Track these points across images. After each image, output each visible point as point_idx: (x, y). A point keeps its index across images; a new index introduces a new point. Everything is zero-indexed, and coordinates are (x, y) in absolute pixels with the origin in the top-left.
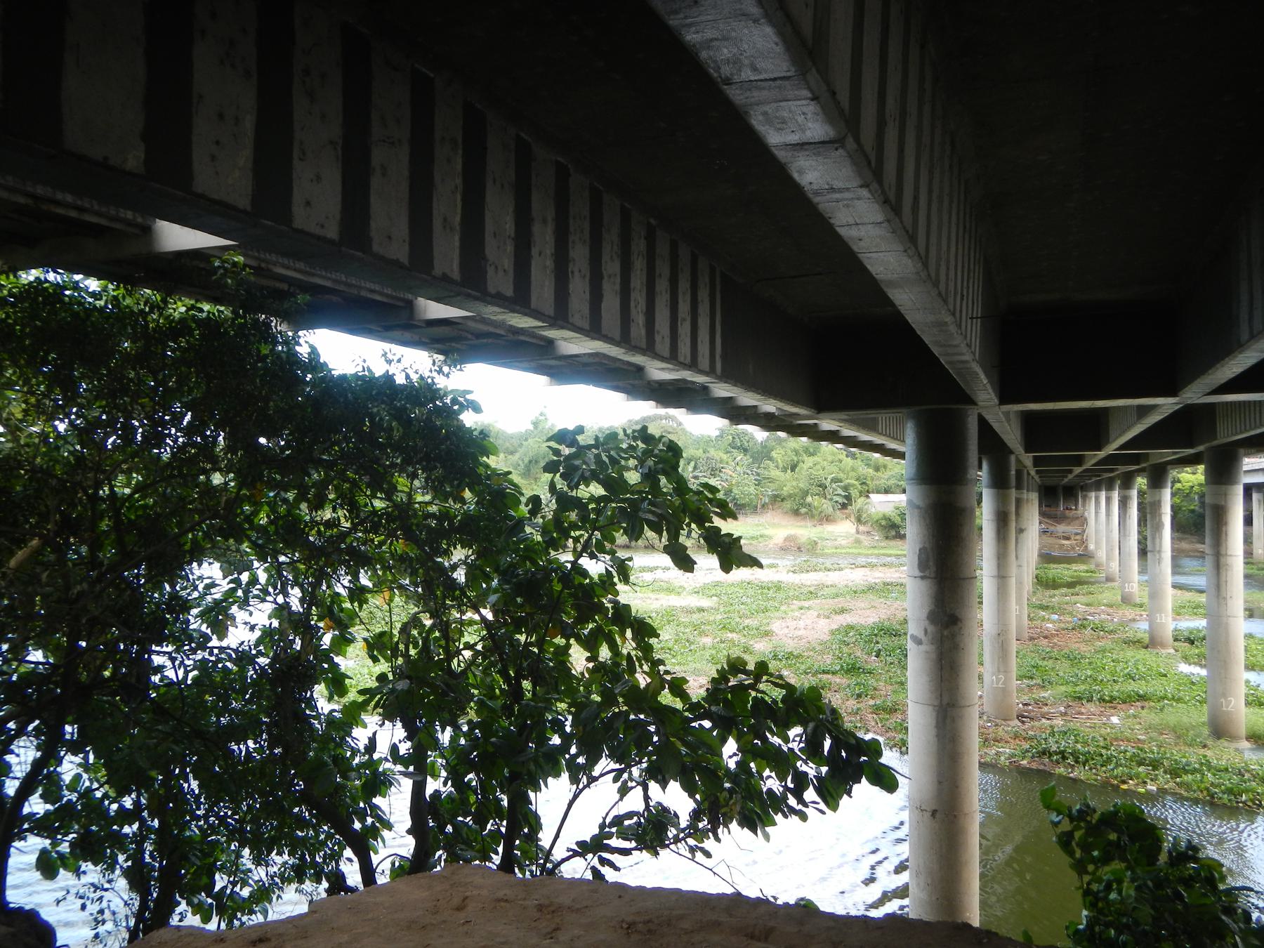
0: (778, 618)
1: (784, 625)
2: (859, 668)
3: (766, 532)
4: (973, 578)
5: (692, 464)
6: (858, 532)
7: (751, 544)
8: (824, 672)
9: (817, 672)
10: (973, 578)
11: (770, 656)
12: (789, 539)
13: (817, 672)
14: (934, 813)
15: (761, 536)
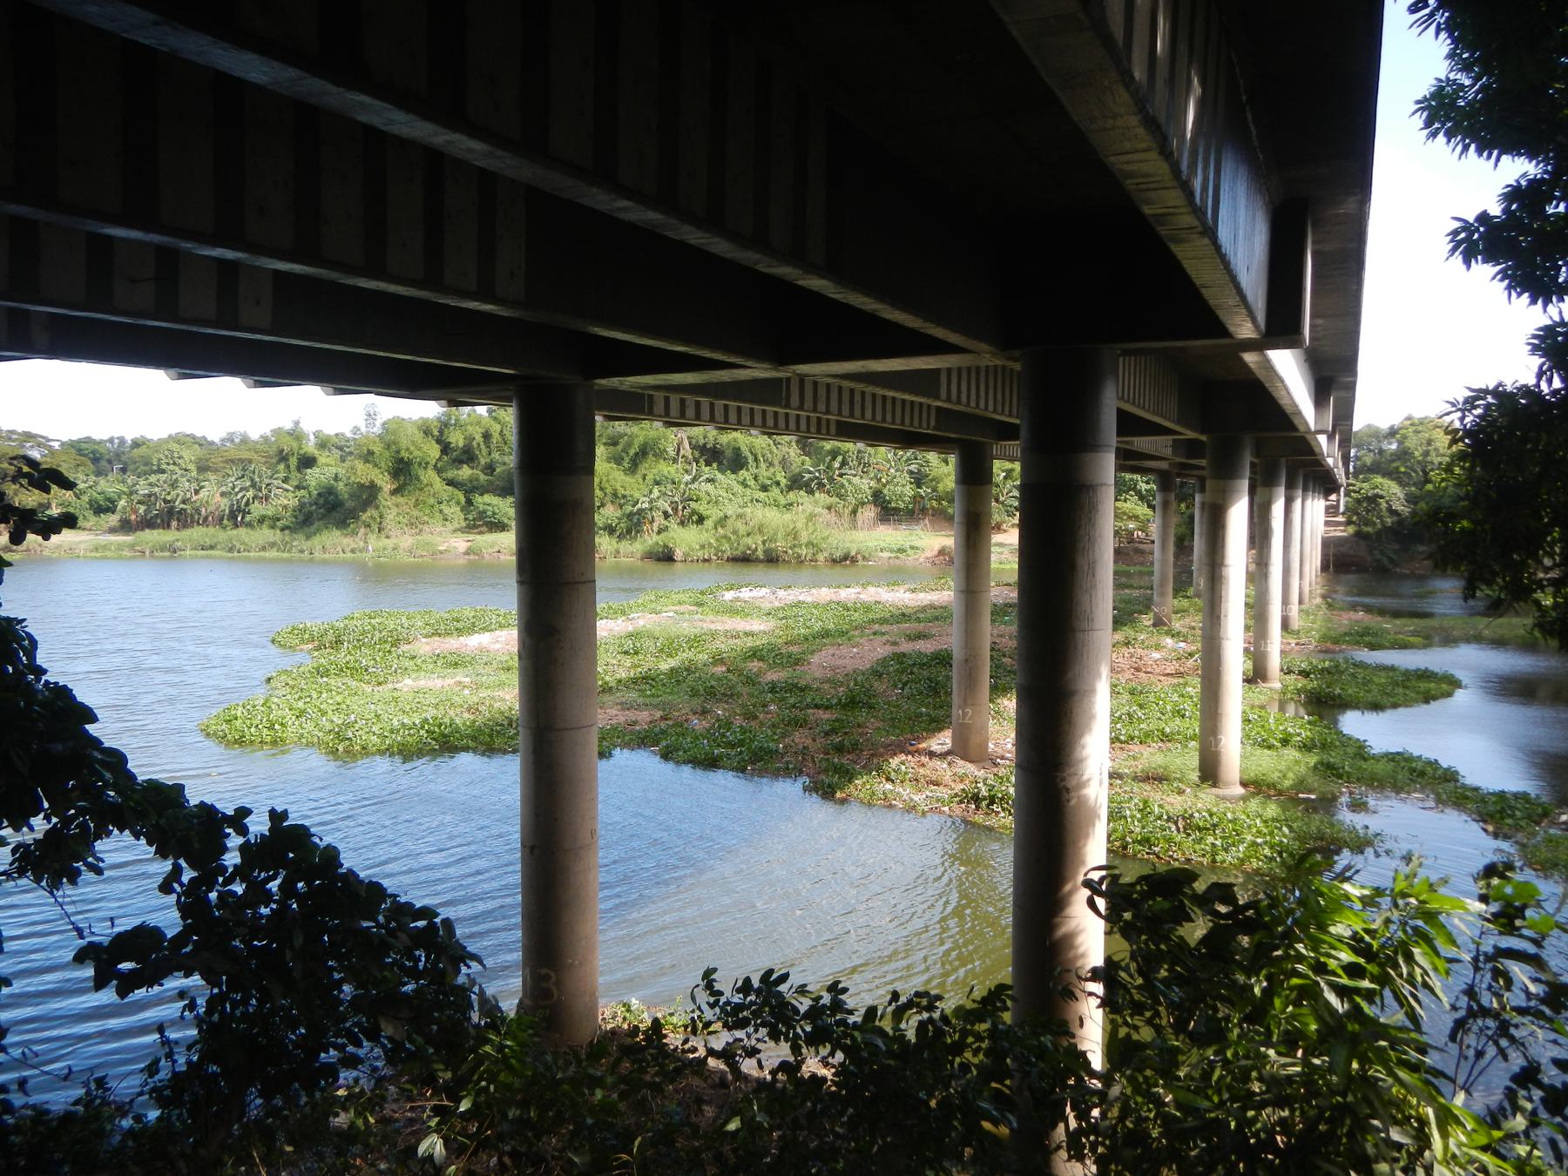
0: (833, 645)
1: (831, 652)
2: (859, 702)
3: (917, 544)
4: (579, 583)
5: (840, 458)
7: (898, 558)
8: (817, 707)
9: (808, 706)
10: (579, 583)
11: (766, 688)
12: (942, 552)
13: (808, 706)
14: (532, 848)
15: (912, 548)
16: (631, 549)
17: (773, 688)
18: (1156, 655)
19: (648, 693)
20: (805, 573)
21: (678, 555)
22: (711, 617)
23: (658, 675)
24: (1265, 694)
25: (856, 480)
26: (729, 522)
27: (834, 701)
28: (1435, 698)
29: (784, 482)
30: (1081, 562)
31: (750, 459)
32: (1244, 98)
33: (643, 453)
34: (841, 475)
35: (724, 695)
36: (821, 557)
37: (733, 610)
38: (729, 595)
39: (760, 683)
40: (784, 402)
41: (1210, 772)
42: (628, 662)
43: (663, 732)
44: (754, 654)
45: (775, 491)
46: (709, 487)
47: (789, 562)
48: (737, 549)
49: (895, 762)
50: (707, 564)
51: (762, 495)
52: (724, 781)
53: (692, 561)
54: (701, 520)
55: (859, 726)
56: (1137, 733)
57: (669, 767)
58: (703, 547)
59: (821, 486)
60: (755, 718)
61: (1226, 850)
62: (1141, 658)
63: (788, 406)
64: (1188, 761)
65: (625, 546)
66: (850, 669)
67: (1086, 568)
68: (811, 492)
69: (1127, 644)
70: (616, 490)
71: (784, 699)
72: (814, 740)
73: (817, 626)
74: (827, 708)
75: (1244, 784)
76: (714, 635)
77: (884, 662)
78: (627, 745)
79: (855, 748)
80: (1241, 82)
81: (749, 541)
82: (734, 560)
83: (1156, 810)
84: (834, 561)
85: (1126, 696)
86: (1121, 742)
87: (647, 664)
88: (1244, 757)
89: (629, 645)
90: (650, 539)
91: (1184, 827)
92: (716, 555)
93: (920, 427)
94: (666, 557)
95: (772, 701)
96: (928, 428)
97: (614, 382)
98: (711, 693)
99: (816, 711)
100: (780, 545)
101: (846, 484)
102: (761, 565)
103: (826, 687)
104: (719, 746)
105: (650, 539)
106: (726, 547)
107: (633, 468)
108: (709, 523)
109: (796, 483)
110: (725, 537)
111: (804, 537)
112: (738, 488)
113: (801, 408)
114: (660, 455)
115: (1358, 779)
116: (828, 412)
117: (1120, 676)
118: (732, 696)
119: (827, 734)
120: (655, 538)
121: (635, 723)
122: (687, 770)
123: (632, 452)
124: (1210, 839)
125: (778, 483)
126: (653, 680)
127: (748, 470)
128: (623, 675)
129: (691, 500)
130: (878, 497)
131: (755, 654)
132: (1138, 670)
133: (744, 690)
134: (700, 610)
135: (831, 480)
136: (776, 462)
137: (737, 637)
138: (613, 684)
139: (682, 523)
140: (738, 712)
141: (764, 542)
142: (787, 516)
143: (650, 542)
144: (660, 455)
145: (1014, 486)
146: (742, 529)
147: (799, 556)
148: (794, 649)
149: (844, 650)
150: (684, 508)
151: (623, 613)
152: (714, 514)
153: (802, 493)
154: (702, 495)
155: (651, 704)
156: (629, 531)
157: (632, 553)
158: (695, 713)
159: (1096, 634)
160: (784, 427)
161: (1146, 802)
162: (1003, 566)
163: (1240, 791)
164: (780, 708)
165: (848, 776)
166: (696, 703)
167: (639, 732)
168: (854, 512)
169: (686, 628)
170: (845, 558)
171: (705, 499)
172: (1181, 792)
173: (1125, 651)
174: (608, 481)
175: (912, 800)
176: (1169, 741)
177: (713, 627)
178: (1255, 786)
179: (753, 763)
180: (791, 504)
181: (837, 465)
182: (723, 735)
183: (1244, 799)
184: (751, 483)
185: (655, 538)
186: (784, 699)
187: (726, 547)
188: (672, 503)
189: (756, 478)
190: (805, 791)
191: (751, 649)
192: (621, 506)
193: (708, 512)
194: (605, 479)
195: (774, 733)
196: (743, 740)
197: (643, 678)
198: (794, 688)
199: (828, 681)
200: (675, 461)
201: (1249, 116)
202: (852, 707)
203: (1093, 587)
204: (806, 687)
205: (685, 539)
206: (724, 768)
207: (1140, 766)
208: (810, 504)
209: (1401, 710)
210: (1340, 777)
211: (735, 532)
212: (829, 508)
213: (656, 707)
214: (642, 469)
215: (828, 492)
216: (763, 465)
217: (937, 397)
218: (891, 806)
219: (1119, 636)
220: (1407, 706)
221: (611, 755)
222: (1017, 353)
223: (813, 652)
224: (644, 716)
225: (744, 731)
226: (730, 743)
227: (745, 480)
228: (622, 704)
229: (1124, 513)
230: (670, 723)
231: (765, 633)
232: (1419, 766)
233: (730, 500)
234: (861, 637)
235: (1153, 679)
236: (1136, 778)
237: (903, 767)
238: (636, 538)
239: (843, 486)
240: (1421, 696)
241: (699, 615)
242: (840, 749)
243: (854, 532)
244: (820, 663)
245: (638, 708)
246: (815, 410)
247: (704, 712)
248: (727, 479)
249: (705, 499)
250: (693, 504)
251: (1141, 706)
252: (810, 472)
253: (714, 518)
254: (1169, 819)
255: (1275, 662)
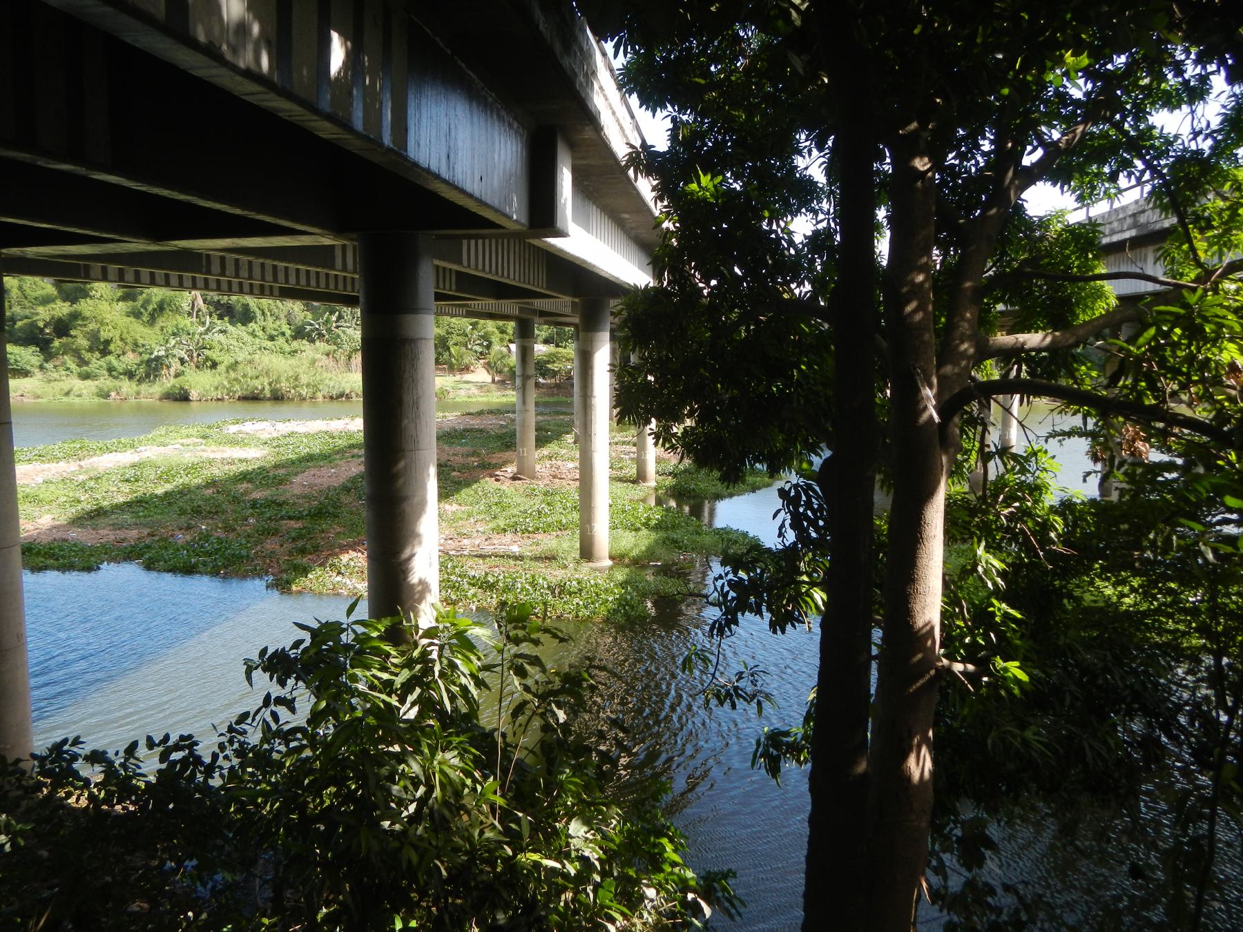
1: (312, 473)
6: (493, 381)
8: (290, 518)
9: (282, 518)
16: (151, 390)
17: (254, 504)
18: (571, 465)
19: (141, 514)
20: (306, 406)
21: (194, 394)
22: (213, 447)
23: (152, 498)
24: (644, 491)
25: (350, 331)
26: (240, 367)
27: (306, 512)
28: (759, 488)
29: (288, 333)
30: (407, 398)
31: (258, 313)
32: (449, 52)
33: (161, 308)
34: (337, 327)
35: (210, 512)
36: (320, 395)
37: (233, 442)
38: (233, 429)
39: (244, 501)
40: (204, 270)
41: (587, 552)
42: (126, 488)
43: (148, 547)
44: (245, 477)
45: (281, 340)
46: (221, 337)
47: (292, 400)
48: (247, 390)
49: (345, 558)
50: (220, 403)
51: (269, 344)
52: (202, 587)
53: (206, 400)
54: (214, 365)
55: (323, 531)
56: (541, 525)
57: (154, 574)
58: (217, 388)
59: (321, 336)
60: (234, 530)
61: (586, 607)
62: (558, 469)
63: (209, 272)
64: (569, 544)
65: (144, 387)
66: (325, 486)
67: (411, 403)
68: (312, 341)
69: (550, 458)
70: (136, 340)
71: (262, 513)
72: (282, 546)
73: (304, 451)
74: (299, 519)
75: (612, 558)
76: (211, 462)
77: (353, 480)
78: (114, 560)
79: (316, 549)
80: (437, 39)
81: (257, 383)
82: (244, 398)
83: (541, 581)
84: (331, 398)
85: (541, 497)
86: (529, 532)
87: (142, 489)
88: (613, 539)
89: (130, 473)
90: (167, 382)
91: (560, 593)
92: (228, 395)
93: (345, 290)
94: (183, 397)
95: (252, 515)
96: (353, 291)
97: (15, 251)
98: (197, 511)
99: (288, 521)
100: (284, 385)
101: (342, 335)
102: (268, 405)
103: (301, 501)
104: (197, 555)
105: (167, 382)
106: (237, 387)
107: (152, 320)
108: (221, 368)
110: (236, 379)
111: (304, 379)
113: (223, 274)
114: (178, 310)
115: (693, 549)
116: (250, 278)
117: (540, 483)
118: (217, 512)
119: (294, 540)
120: (173, 381)
121: (124, 540)
122: (168, 577)
123: (150, 308)
124: (576, 600)
125: (283, 334)
126: (147, 503)
127: (256, 322)
128: (121, 499)
129: (205, 348)
131: (245, 477)
132: (554, 477)
133: (229, 508)
134: (204, 442)
135: (329, 331)
136: (282, 316)
137: (232, 463)
138: (108, 508)
139: (197, 367)
140: (220, 525)
141: (270, 384)
142: (293, 361)
143: (169, 385)
144: (178, 310)
145: (482, 337)
146: (250, 372)
147: (300, 395)
148: (281, 472)
149: (324, 471)
150: (199, 355)
151: (132, 446)
152: (227, 360)
153: (304, 342)
154: (215, 344)
155: (141, 524)
156: (148, 376)
157: (151, 394)
158: (181, 529)
159: (421, 452)
160: (227, 289)
161: (533, 577)
162: (470, 400)
163: (610, 563)
164: (257, 521)
165: (305, 571)
166: (183, 520)
167: (126, 548)
168: (350, 357)
169: (188, 458)
170: (341, 395)
171: (218, 347)
172: (565, 567)
173: (548, 463)
174: (128, 333)
175: (355, 588)
176: (565, 529)
177: (212, 456)
178: (617, 558)
179: (226, 567)
180: (296, 351)
181: (334, 318)
182: (202, 547)
183: (611, 568)
184: (260, 333)
185: (173, 381)
186: (262, 513)
187: (237, 387)
188: (187, 351)
189: (264, 329)
190: (267, 587)
191: (241, 473)
192: (141, 354)
193: (221, 359)
194: (125, 331)
195: (248, 542)
196: (220, 549)
197: (138, 502)
198: (272, 503)
199: (305, 497)
200: (190, 314)
201: (463, 65)
202: (320, 518)
203: (418, 417)
204: (284, 502)
205: (199, 382)
206: (201, 573)
207: (538, 551)
208: (311, 351)
209: (735, 498)
210: (680, 548)
211: (245, 376)
212: (328, 355)
213: (145, 526)
214: (161, 322)
215: (327, 342)
216: (270, 319)
217: (333, 268)
218: (338, 594)
219: (545, 451)
220: (739, 495)
221: (99, 568)
222: (354, 236)
223: (296, 474)
224: (134, 533)
225: (219, 540)
226: (207, 552)
227: (254, 331)
228: (113, 525)
229: (563, 357)
230: (156, 538)
231: (258, 459)
232: (733, 537)
233: (241, 348)
234: (341, 459)
235: (564, 482)
236: (537, 559)
237: (352, 563)
238: (154, 382)
239: (339, 336)
240: (750, 487)
241: (203, 447)
242: (303, 551)
243: (349, 374)
244: (300, 483)
245: (129, 527)
246: (237, 276)
247: (189, 528)
248: (237, 331)
249: (218, 347)
250: (207, 352)
251: (548, 504)
252: (311, 325)
253: (226, 363)
254: (549, 588)
255: (651, 468)
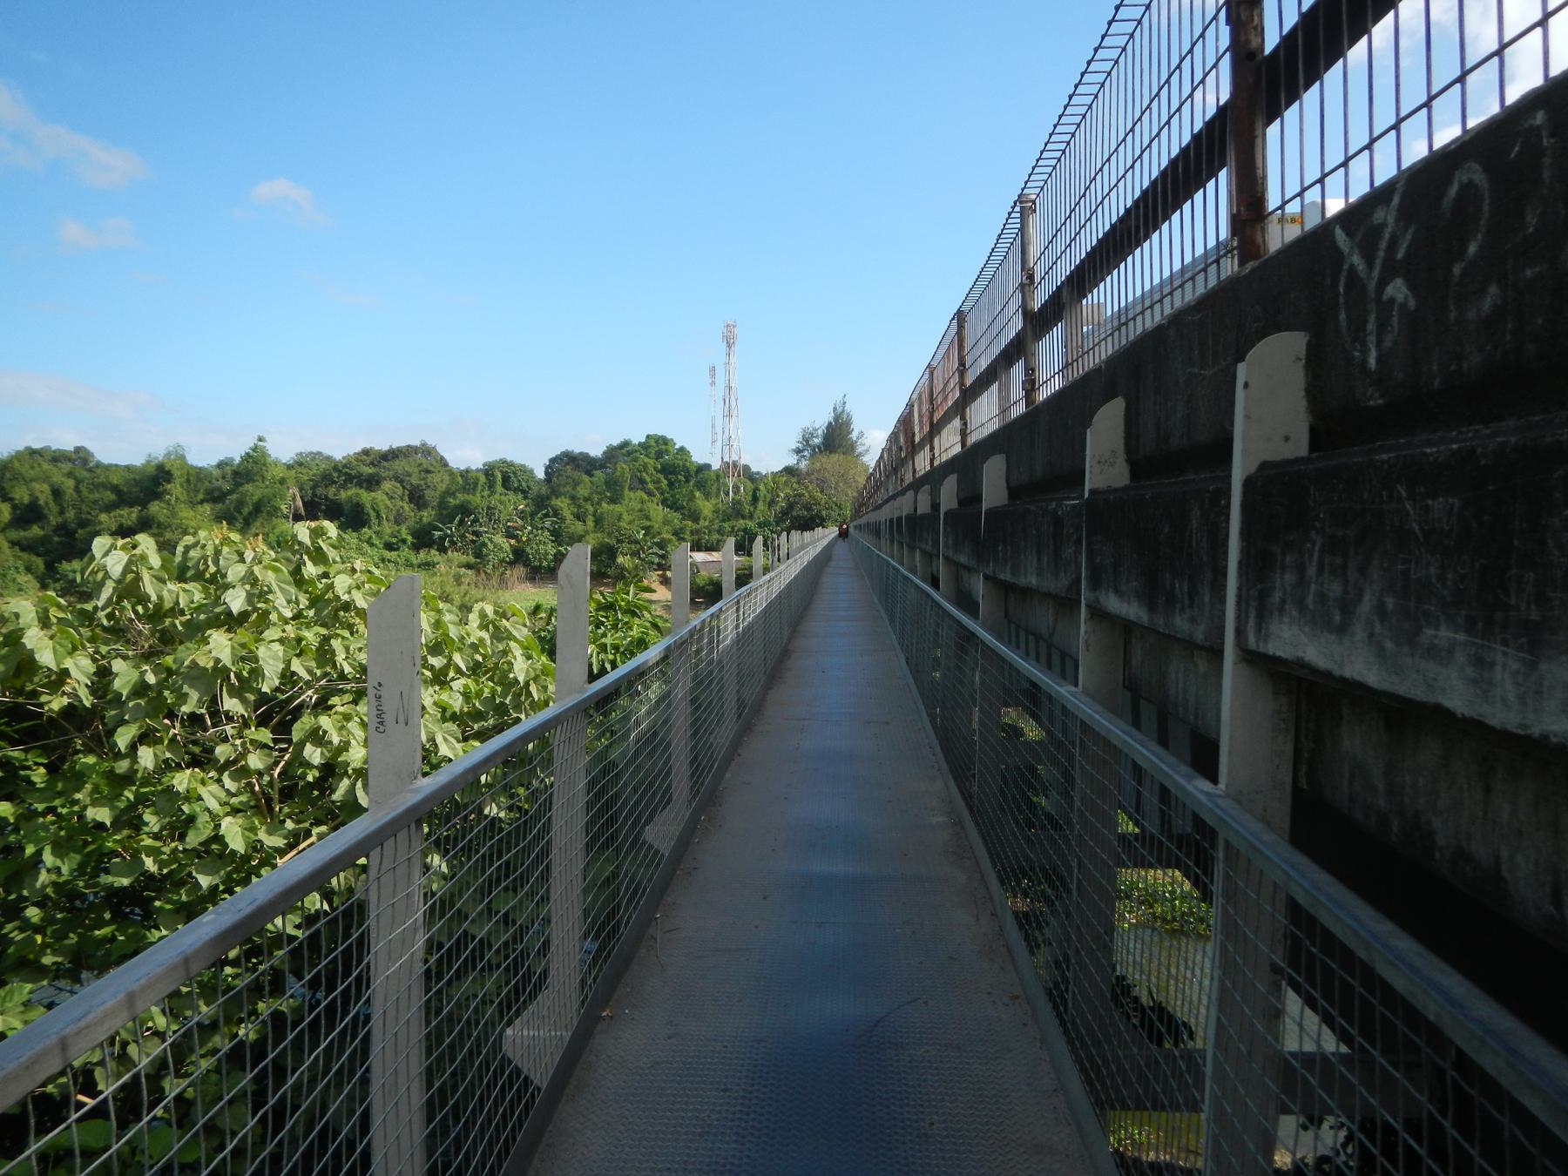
45: (405, 552)
68: (442, 550)
109: (423, 539)
112: (365, 545)
123: (246, 511)
125: (404, 541)
127: (370, 528)
130: (519, 556)
153: (433, 552)
168: (503, 574)
216: (385, 522)
227: (370, 538)
239: (484, 545)
